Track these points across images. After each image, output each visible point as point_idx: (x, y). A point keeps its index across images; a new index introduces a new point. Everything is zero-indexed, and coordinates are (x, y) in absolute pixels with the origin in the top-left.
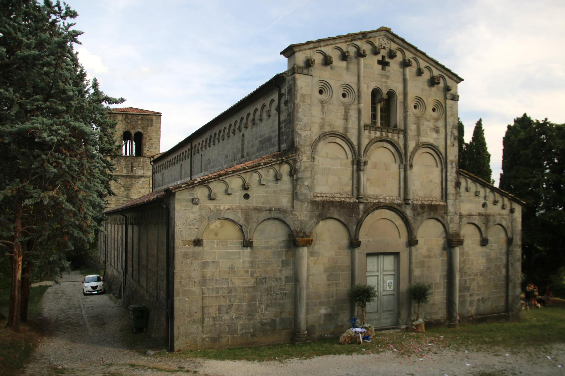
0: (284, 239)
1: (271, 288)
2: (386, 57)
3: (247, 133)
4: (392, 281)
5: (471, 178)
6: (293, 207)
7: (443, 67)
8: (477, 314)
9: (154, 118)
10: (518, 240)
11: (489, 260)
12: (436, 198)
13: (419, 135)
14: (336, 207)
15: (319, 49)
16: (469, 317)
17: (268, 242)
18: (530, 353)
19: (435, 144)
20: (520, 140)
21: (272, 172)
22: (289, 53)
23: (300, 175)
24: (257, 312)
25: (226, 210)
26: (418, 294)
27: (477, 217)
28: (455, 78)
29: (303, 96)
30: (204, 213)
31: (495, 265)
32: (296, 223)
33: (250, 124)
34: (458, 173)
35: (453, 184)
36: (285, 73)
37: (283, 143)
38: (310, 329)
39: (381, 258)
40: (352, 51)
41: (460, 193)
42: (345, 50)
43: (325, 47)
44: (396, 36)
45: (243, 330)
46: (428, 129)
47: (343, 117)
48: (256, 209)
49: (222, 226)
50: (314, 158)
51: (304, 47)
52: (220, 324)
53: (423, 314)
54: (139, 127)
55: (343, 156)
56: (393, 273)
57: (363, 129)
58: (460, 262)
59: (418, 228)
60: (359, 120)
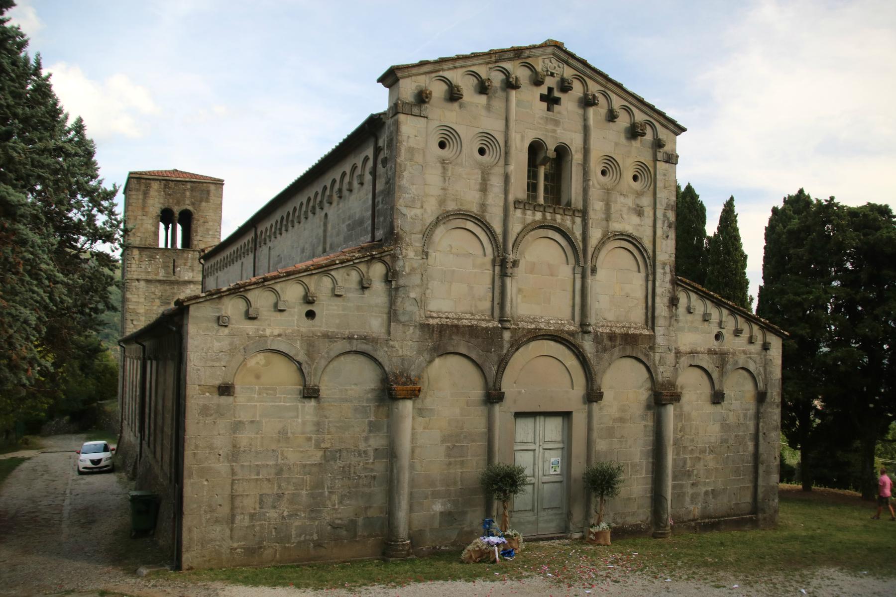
0: (373, 386)
1: (349, 467)
2: (555, 90)
3: (332, 211)
4: (559, 459)
5: (696, 291)
6: (389, 333)
7: (651, 108)
8: (703, 517)
9: (212, 187)
10: (775, 394)
11: (725, 426)
12: (635, 324)
13: (608, 219)
14: (463, 334)
15: (441, 73)
16: (689, 520)
17: (346, 390)
18: (775, 584)
19: (635, 234)
20: (791, 232)
21: (354, 276)
22: (389, 81)
23: (402, 282)
24: (325, 506)
25: (275, 336)
26: (601, 482)
27: (706, 357)
28: (671, 127)
29: (411, 150)
30: (237, 341)
31: (736, 436)
32: (394, 360)
33: (335, 197)
34: (674, 283)
35: (666, 300)
36: (384, 113)
37: (378, 229)
38: (415, 538)
39: (540, 420)
40: (497, 78)
41: (676, 316)
42: (484, 76)
43: (451, 72)
44: (572, 56)
45: (300, 536)
46: (625, 210)
47: (478, 187)
48: (326, 336)
49: (268, 364)
50: (427, 254)
51: (414, 71)
52: (261, 526)
53: (612, 515)
54: (188, 202)
55: (476, 249)
56: (561, 446)
57: (511, 208)
58: (675, 429)
59: (604, 372)
60: (506, 192)
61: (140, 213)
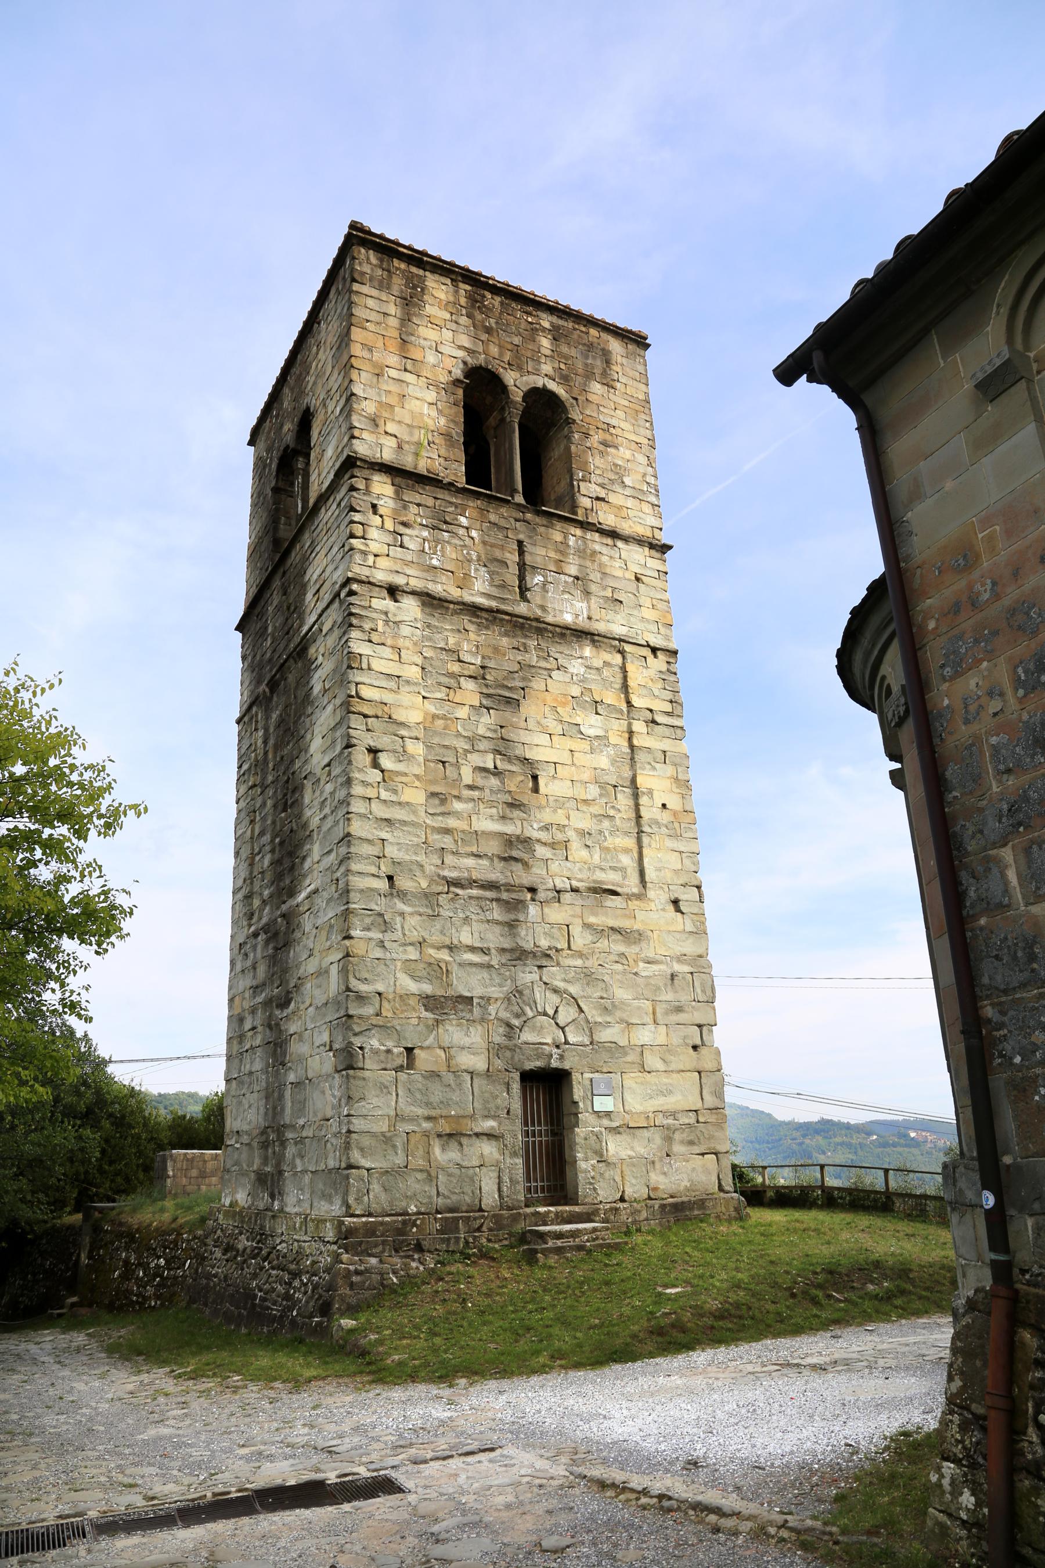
9: (615, 346)
54: (547, 368)
61: (393, 360)
